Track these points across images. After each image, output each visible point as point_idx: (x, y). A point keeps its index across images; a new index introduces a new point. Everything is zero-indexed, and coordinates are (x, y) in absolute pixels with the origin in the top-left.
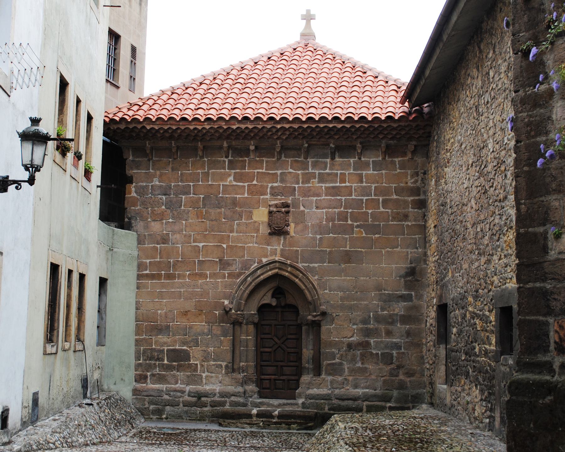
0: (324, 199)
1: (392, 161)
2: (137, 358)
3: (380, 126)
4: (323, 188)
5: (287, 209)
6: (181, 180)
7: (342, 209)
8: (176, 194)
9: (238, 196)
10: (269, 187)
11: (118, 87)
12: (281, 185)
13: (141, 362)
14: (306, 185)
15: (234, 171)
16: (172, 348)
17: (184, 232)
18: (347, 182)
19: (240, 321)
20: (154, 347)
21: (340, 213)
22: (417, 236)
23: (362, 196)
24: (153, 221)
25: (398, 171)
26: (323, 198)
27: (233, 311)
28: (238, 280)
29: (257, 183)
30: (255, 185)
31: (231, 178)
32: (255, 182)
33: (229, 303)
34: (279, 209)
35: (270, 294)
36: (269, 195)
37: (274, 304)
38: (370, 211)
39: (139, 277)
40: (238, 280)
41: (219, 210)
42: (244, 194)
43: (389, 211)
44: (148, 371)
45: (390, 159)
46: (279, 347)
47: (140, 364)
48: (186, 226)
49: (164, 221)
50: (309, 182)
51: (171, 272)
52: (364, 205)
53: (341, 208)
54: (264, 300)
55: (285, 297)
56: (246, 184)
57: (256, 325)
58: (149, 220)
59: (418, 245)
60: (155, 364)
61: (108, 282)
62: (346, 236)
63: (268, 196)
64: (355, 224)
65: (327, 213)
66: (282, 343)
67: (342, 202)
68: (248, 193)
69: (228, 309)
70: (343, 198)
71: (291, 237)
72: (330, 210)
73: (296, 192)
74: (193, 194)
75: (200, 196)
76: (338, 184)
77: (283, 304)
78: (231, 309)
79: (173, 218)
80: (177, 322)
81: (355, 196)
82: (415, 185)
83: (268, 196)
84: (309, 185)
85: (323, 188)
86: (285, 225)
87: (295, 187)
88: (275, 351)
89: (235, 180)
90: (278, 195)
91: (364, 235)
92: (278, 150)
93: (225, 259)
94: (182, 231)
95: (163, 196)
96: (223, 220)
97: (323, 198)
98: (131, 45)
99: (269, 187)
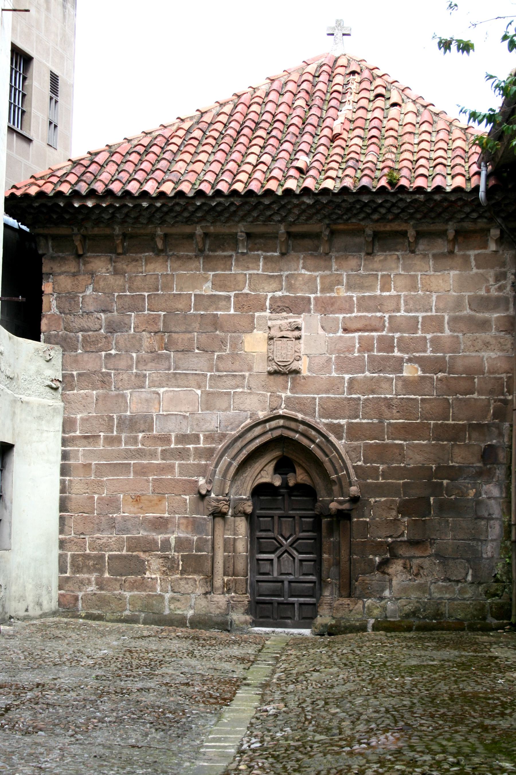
1: (464, 255)
2: (62, 569)
3: (445, 199)
4: (355, 299)
5: (296, 333)
6: (129, 287)
7: (384, 333)
8: (122, 310)
9: (219, 313)
10: (269, 297)
11: (29, 140)
12: (288, 294)
13: (68, 575)
14: (328, 295)
15: (214, 273)
16: (117, 553)
17: (135, 371)
18: (393, 290)
19: (224, 510)
20: (88, 551)
21: (381, 339)
22: (502, 375)
23: (417, 311)
24: (86, 352)
25: (475, 270)
26: (354, 315)
27: (213, 495)
29: (250, 292)
30: (247, 294)
31: (209, 284)
32: (246, 291)
33: (206, 482)
34: (284, 334)
35: (270, 468)
36: (268, 311)
37: (277, 482)
38: (429, 336)
39: (65, 442)
40: (220, 446)
41: (189, 336)
42: (229, 309)
43: (460, 335)
44: (80, 590)
45: (462, 253)
46: (286, 551)
47: (68, 578)
48: (138, 362)
49: (103, 353)
50: (332, 290)
51: (115, 433)
52: (419, 326)
53: (383, 330)
54: (262, 477)
56: (232, 294)
57: (250, 517)
58: (80, 351)
59: (506, 390)
60: (89, 579)
61: (15, 449)
62: (391, 376)
63: (267, 313)
64: (406, 356)
65: (360, 338)
66: (291, 546)
67: (384, 321)
69: (204, 492)
70: (387, 315)
71: (304, 378)
72: (366, 334)
73: (312, 306)
74: (148, 310)
75: (160, 312)
76: (378, 293)
77: (291, 483)
78: (209, 492)
79: (117, 349)
80: (124, 513)
81: (406, 311)
82: (501, 294)
83: (267, 313)
84: (333, 295)
85: (355, 299)
86: (295, 359)
87: (309, 298)
89: (215, 286)
90: (283, 310)
91: (420, 373)
92: (283, 240)
93: (200, 412)
94: (130, 367)
95: (102, 314)
96: (197, 351)
97: (354, 315)
98: (50, 73)
99: (269, 297)
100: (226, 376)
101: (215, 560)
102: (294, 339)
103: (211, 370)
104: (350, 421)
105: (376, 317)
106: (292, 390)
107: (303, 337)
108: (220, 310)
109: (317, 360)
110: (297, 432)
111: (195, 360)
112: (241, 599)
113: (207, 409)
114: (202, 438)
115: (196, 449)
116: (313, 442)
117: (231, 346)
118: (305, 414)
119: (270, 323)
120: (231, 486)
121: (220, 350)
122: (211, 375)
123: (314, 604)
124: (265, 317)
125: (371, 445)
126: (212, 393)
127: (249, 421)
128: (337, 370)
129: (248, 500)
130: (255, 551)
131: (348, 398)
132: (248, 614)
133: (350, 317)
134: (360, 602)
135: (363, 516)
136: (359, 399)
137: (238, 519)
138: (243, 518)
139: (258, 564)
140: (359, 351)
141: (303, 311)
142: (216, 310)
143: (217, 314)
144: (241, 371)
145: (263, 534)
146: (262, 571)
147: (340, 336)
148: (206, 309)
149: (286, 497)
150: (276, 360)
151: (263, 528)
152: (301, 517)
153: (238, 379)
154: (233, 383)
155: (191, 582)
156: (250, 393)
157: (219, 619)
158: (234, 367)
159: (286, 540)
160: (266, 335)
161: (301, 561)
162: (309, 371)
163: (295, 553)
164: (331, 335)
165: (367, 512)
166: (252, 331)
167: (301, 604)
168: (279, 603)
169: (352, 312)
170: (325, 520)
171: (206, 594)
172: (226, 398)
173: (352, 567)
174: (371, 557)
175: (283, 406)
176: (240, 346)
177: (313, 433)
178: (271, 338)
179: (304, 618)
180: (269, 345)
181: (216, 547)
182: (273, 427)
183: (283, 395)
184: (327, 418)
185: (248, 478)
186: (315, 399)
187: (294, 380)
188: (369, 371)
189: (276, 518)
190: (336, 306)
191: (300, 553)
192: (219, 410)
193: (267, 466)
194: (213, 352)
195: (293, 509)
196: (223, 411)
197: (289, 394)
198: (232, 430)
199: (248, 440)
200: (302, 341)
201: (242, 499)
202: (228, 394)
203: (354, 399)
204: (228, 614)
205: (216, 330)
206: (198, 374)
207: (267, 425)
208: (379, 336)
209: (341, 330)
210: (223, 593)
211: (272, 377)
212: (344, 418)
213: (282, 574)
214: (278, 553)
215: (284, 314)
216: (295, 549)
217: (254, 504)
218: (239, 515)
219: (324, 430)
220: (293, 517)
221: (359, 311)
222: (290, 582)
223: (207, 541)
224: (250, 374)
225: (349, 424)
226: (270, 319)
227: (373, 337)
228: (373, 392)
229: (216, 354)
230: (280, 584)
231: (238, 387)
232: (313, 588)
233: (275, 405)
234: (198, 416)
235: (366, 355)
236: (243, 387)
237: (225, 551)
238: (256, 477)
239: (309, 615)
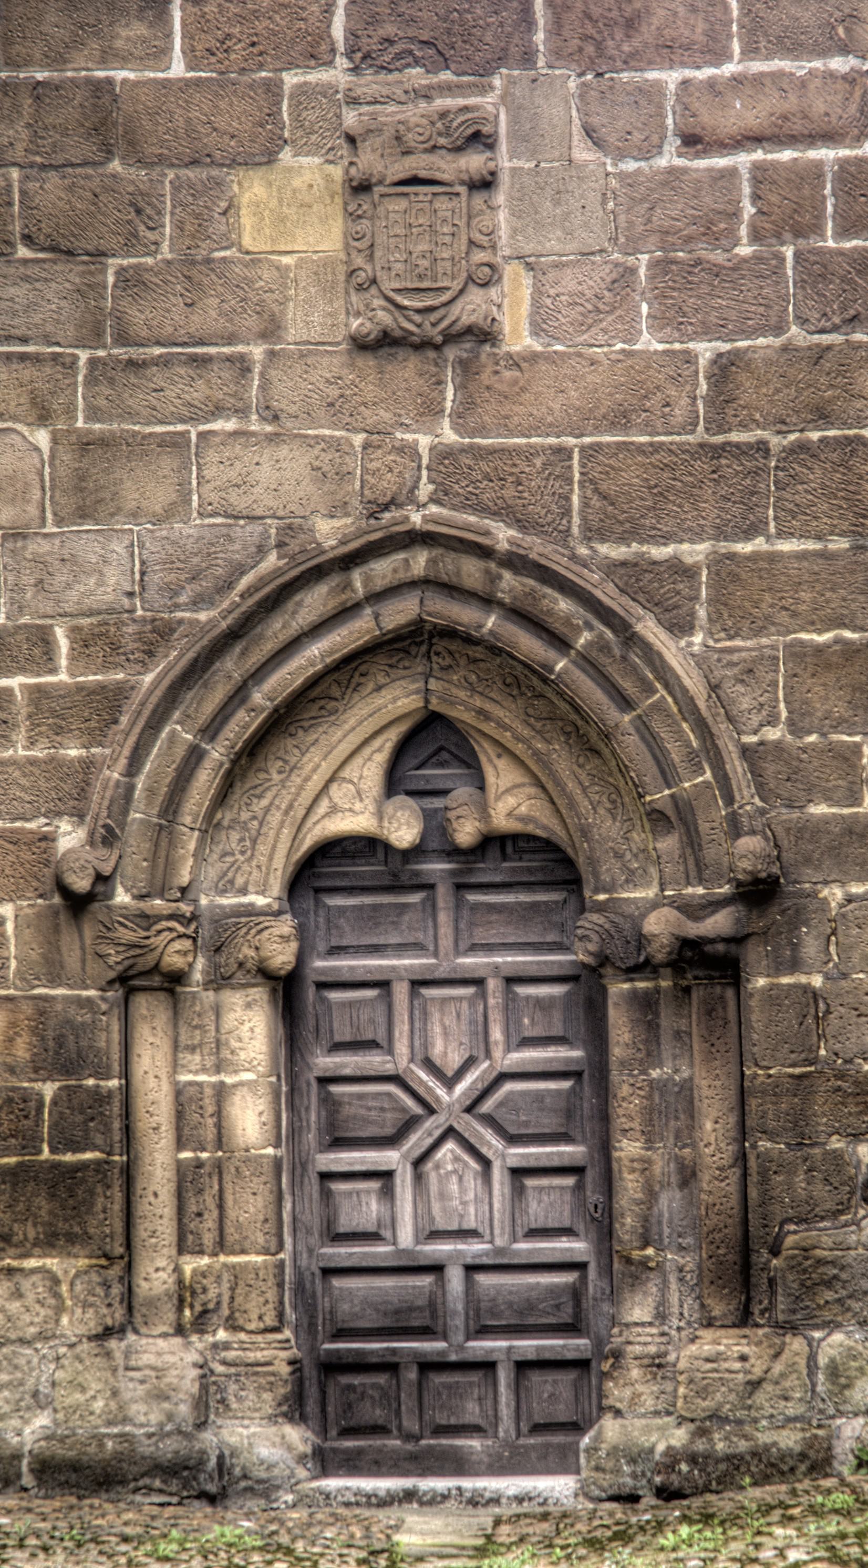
0: (737, 80)
9: (121, 75)
19: (173, 960)
27: (122, 897)
28: (148, 678)
33: (91, 841)
34: (417, 164)
36: (342, 62)
40: (148, 678)
42: (161, 54)
46: (450, 1132)
54: (334, 810)
55: (482, 787)
66: (469, 1110)
68: (189, 52)
69: (81, 883)
71: (515, 362)
72: (786, 155)
73: (540, 37)
86: (470, 279)
88: (418, 1162)
90: (405, 58)
93: (51, 529)
96: (23, 252)
97: (729, 69)
100: (164, 362)
101: (139, 1185)
102: (462, 190)
103: (94, 337)
104: (724, 547)
105: (831, 75)
106: (459, 419)
107: (505, 179)
108: (124, 60)
109: (569, 282)
110: (487, 601)
111: (20, 292)
112: (259, 1356)
113: (83, 514)
114: (63, 643)
115: (38, 694)
116: (561, 643)
117: (179, 226)
118: (522, 524)
119: (350, 118)
120: (198, 855)
121: (132, 242)
122: (93, 362)
123: (582, 1365)
124: (327, 91)
125: (819, 650)
126: (104, 442)
127: (272, 560)
128: (659, 322)
129: (279, 913)
130: (311, 1138)
131: (714, 447)
132: (289, 1418)
133: (711, 84)
134: (796, 1344)
135: (795, 965)
136: (762, 447)
137: (234, 1000)
138: (259, 993)
139: (327, 1196)
140: (756, 236)
141: (502, 59)
142: (107, 57)
143: (109, 81)
144: (231, 340)
145: (349, 1062)
146: (345, 1224)
147: (672, 171)
148: (57, 60)
149: (443, 893)
150: (388, 285)
151: (344, 1034)
152: (511, 981)
153: (221, 375)
154: (198, 393)
155: (34, 1288)
156: (272, 438)
157: (169, 1448)
158: (198, 322)
159: (450, 1082)
160: (337, 172)
161: (518, 1173)
162: (537, 330)
163: (491, 1143)
164: (630, 166)
165: (810, 948)
166: (270, 158)
167: (523, 1367)
168: (428, 1366)
169: (720, 55)
170: (618, 988)
171: (108, 1333)
172: (167, 463)
173: (753, 1193)
174: (836, 1143)
175: (425, 490)
176: (219, 226)
177: (564, 605)
178: (361, 188)
179: (537, 1428)
180: (353, 217)
181: (143, 1123)
182: (379, 584)
183: (424, 442)
184: (623, 539)
185: (275, 818)
186: (563, 453)
187: (467, 368)
188: (802, 321)
189: (401, 991)
190: (647, 33)
191: (513, 1139)
192: (135, 515)
193: (358, 761)
194: (100, 254)
195: (473, 948)
196: (158, 520)
197: (449, 436)
198: (197, 603)
199: (269, 647)
200: (500, 198)
201: (250, 911)
202: (177, 443)
203: (740, 450)
204: (201, 1425)
205: (109, 154)
206: (36, 359)
207: (357, 578)
208: (844, 163)
209: (672, 143)
210: (180, 1330)
211: (368, 362)
212: (697, 536)
213: (436, 1235)
214: (417, 1141)
215: (416, 76)
216: (490, 1120)
217: (302, 932)
218: (240, 978)
219: (607, 594)
220: (479, 982)
221: (750, 51)
222: (471, 1269)
223: (100, 1098)
224: (272, 354)
225: (719, 562)
226: (353, 101)
227: (817, 168)
228: (822, 416)
229: (114, 263)
230: (425, 1281)
231: (218, 411)
232: (576, 1293)
233: (387, 485)
234: (44, 547)
235: (789, 252)
236: (242, 412)
237: (180, 1143)
238: (309, 810)
239: (562, 1413)
